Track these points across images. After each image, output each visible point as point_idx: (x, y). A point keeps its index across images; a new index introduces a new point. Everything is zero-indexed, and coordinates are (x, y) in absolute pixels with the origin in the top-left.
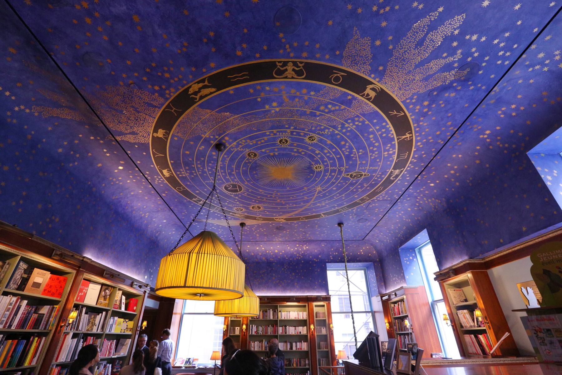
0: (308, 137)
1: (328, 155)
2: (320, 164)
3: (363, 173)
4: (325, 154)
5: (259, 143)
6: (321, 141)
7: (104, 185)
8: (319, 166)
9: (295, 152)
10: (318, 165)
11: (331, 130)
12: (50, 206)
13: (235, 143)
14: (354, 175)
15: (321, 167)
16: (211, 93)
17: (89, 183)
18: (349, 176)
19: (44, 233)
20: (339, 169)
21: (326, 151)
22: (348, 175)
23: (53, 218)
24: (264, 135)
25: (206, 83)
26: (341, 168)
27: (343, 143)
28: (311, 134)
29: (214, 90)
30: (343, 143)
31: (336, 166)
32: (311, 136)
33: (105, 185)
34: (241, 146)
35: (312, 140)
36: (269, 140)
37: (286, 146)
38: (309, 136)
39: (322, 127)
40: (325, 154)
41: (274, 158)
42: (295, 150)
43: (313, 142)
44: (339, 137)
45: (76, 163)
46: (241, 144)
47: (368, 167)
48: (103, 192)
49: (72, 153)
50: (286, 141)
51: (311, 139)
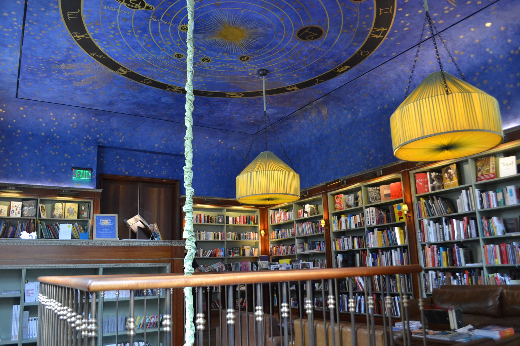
0: (182, 58)
1: (167, 39)
2: (181, 32)
3: (125, 5)
4: (171, 40)
5: (228, 65)
6: (171, 52)
7: (387, 96)
8: (184, 30)
9: (201, 50)
10: (183, 31)
11: (159, 58)
12: (364, 148)
13: (249, 70)
14: (139, 5)
15: (181, 28)
16: (230, 93)
17: (379, 107)
18: (146, 5)
19: (370, 165)
20: (160, 19)
21: (169, 43)
22: (148, 7)
23: (370, 152)
24: (217, 68)
25: (228, 96)
26: (155, 20)
27: (149, 46)
28: (178, 60)
29: (227, 94)
30: (149, 46)
31: (162, 24)
32: (178, 58)
33: (389, 95)
34: (246, 67)
35: (179, 55)
36: (218, 64)
37: (206, 57)
38: (180, 58)
39: (166, 61)
40: (171, 40)
41: (227, 51)
42: (200, 51)
43: (179, 54)
44: (152, 51)
45: (361, 110)
46: (244, 68)
47: (119, 11)
48: (393, 99)
49: (353, 110)
50: (203, 60)
51: (179, 56)
